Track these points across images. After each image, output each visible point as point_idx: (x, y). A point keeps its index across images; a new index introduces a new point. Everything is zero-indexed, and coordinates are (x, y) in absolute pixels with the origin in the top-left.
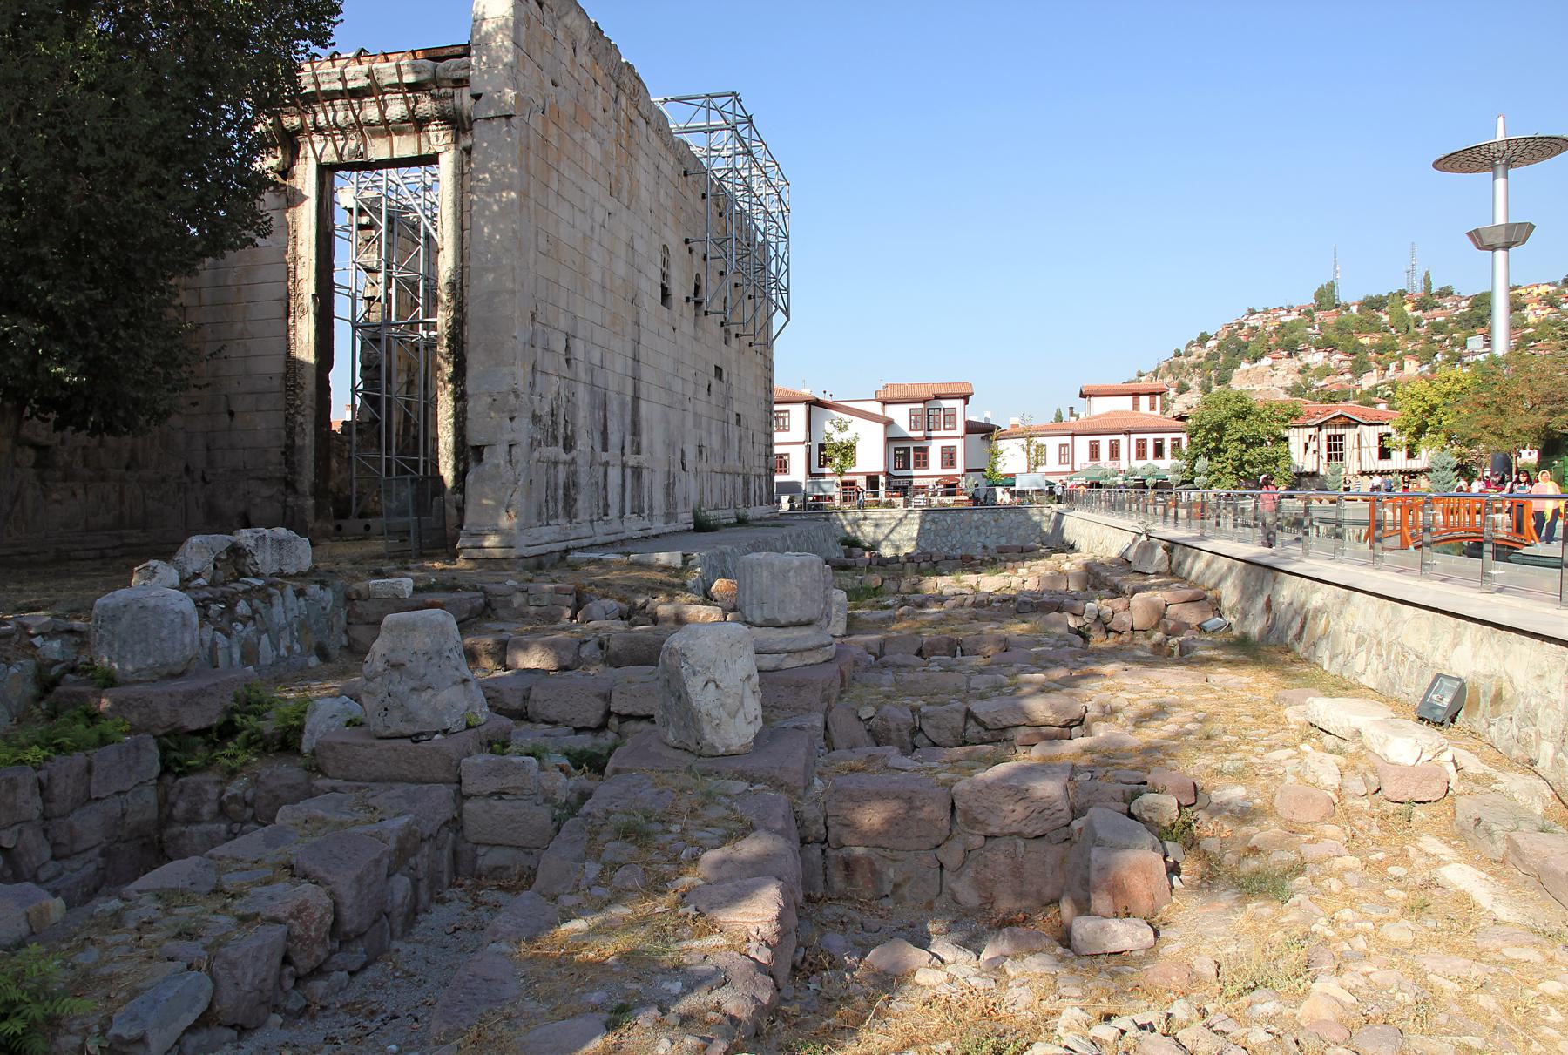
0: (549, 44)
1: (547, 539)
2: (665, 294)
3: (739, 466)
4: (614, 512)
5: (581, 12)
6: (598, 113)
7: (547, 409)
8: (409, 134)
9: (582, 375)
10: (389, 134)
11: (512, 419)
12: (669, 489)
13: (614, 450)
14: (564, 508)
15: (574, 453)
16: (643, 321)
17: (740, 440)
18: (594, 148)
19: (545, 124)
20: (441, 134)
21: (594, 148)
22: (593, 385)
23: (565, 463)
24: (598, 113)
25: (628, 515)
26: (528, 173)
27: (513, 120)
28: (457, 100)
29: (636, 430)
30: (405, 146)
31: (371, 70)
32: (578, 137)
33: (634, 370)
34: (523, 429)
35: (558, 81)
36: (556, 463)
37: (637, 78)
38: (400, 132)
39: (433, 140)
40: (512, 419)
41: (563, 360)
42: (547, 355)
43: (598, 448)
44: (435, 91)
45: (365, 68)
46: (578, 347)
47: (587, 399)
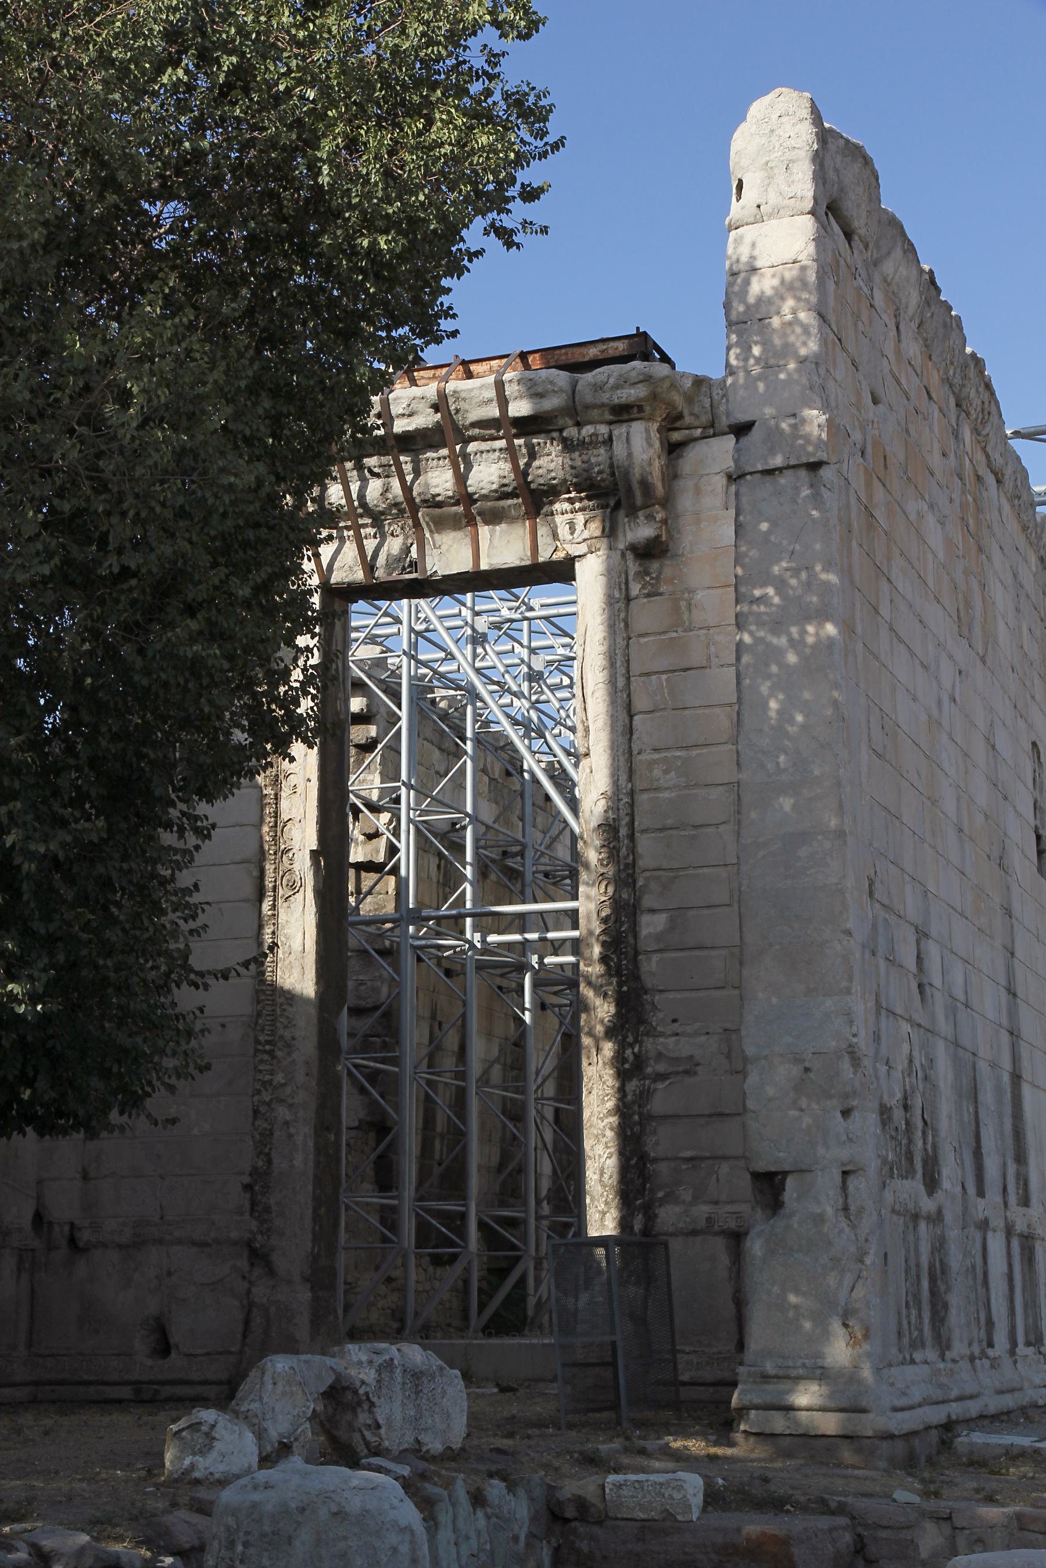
0: (865, 318)
1: (917, 1395)
4: (1001, 1338)
5: (910, 249)
6: (935, 460)
7: (899, 1095)
10: (471, 521)
11: (846, 1113)
13: (993, 1195)
14: (933, 1320)
15: (940, 1195)
18: (935, 537)
19: (868, 484)
20: (580, 518)
21: (935, 537)
22: (957, 1044)
25: (1021, 1349)
26: (852, 582)
27: (826, 473)
28: (619, 449)
30: (504, 546)
31: (442, 396)
32: (912, 507)
34: (865, 1140)
35: (880, 393)
37: (988, 386)
38: (494, 518)
39: (563, 531)
40: (846, 1113)
41: (914, 985)
44: (571, 432)
45: (430, 390)
47: (950, 1076)
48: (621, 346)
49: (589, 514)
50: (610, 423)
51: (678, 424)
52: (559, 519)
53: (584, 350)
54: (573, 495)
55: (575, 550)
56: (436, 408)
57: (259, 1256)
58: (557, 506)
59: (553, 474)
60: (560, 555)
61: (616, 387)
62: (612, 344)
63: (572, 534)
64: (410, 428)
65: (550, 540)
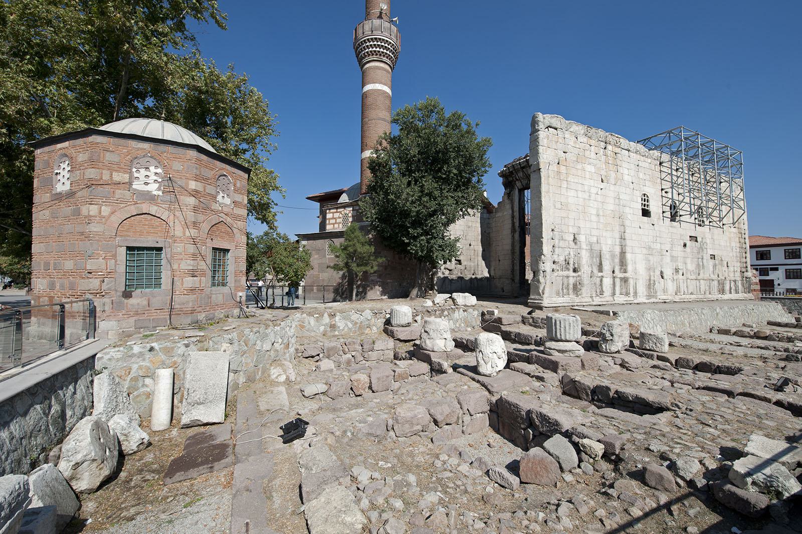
0: (560, 141)
2: (646, 213)
3: (715, 277)
9: (584, 246)
12: (650, 285)
16: (627, 223)
17: (715, 266)
23: (573, 277)
24: (593, 155)
26: (549, 185)
29: (623, 263)
33: (621, 242)
36: (568, 277)
42: (561, 242)
43: (596, 271)
46: (582, 238)
57: (513, 280)
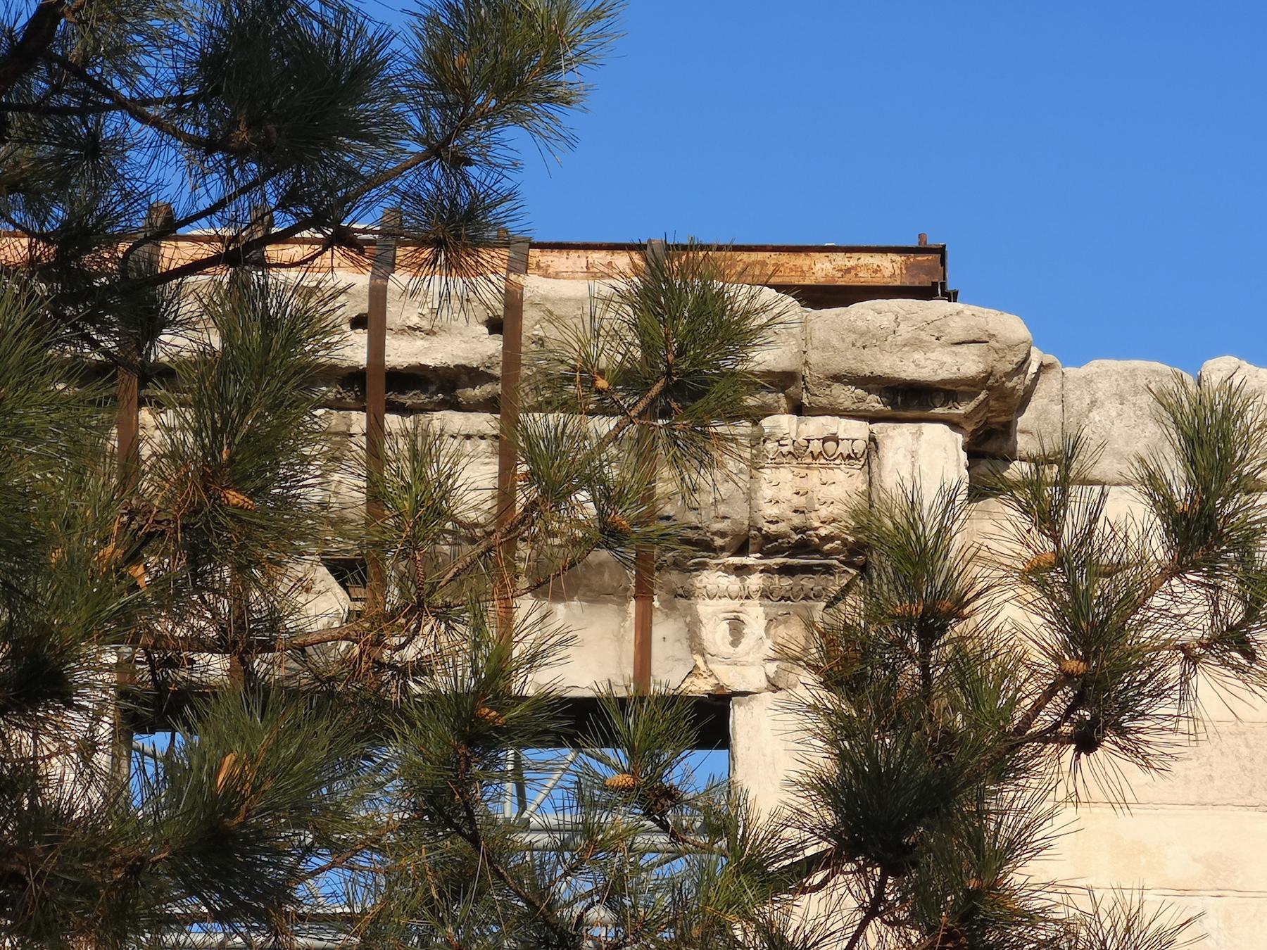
8: (598, 596)
20: (755, 614)
39: (715, 634)
48: (888, 268)
49: (779, 608)
50: (873, 418)
51: (992, 446)
52: (705, 608)
53: (802, 260)
54: (750, 560)
55: (732, 679)
56: (495, 326)
58: (712, 579)
59: (722, 509)
60: (701, 687)
61: (916, 344)
62: (866, 259)
63: (735, 643)
64: (430, 361)
65: (681, 650)
